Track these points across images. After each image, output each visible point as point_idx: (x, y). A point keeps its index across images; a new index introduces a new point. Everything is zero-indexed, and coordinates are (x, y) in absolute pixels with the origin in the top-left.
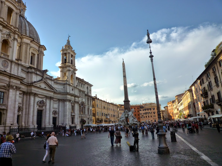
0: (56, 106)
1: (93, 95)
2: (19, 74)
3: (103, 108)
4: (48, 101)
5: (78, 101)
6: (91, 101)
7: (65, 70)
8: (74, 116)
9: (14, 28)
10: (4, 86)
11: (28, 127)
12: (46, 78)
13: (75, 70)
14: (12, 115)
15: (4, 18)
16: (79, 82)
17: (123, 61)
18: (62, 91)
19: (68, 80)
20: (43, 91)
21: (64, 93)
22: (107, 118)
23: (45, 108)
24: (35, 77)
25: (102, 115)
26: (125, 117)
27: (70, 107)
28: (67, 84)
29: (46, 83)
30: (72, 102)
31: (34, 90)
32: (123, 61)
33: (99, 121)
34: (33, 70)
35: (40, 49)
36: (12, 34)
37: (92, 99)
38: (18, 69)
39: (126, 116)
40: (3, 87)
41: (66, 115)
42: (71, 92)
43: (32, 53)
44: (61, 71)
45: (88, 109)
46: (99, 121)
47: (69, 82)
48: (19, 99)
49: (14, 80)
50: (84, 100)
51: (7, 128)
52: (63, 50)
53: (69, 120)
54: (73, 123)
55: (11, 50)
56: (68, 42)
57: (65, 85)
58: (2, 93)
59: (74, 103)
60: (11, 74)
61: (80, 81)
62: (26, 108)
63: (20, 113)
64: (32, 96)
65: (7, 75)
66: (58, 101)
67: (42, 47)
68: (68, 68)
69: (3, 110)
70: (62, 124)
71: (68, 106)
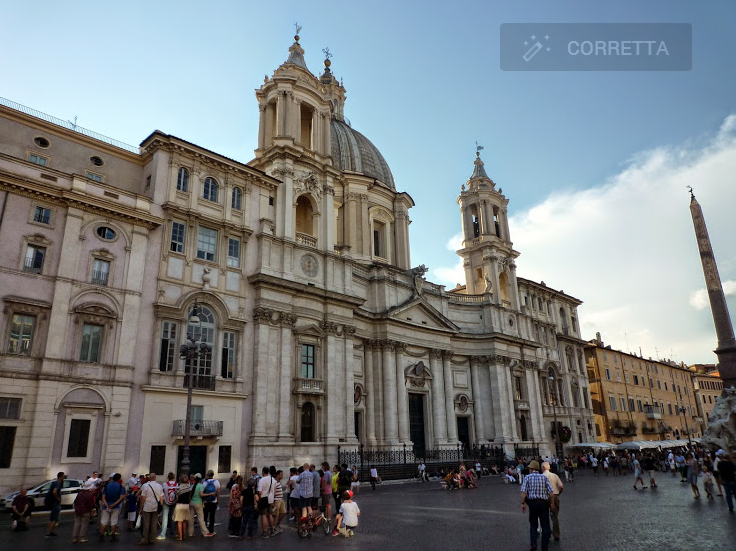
0: (462, 379)
1: (587, 335)
2: (347, 288)
3: (630, 381)
4: (437, 365)
5: (533, 360)
6: (580, 359)
7: (480, 258)
8: (527, 411)
9: (323, 158)
10: (312, 328)
11: (387, 449)
12: (425, 292)
13: (513, 254)
14: (339, 412)
15: (294, 136)
16: (528, 294)
17: (693, 197)
18: (476, 329)
19: (491, 291)
20: (420, 334)
21: (483, 334)
22: (652, 419)
23: (432, 387)
24: (393, 293)
25: (632, 409)
26: (729, 413)
27: (509, 382)
28: (489, 305)
29: (425, 308)
30: (512, 363)
31: (394, 333)
32: (693, 197)
33: (622, 432)
34: (385, 273)
35: (396, 204)
36: (317, 177)
37: (585, 349)
40: (310, 332)
41: (499, 409)
42: (508, 331)
43: (375, 221)
44: (466, 265)
45: (575, 386)
46: (622, 432)
47: (497, 300)
48: (355, 365)
49: (336, 307)
50: (554, 356)
51: (332, 451)
52: (464, 196)
53: (511, 428)
55: (318, 222)
56: (479, 166)
58: (311, 349)
59: (520, 367)
60: (326, 291)
61: (532, 292)
62: (376, 391)
63: (362, 406)
64: (389, 353)
65: (316, 295)
66: (467, 364)
67: (401, 200)
68: (487, 253)
69: (317, 396)
70: (490, 441)
71: (500, 378)
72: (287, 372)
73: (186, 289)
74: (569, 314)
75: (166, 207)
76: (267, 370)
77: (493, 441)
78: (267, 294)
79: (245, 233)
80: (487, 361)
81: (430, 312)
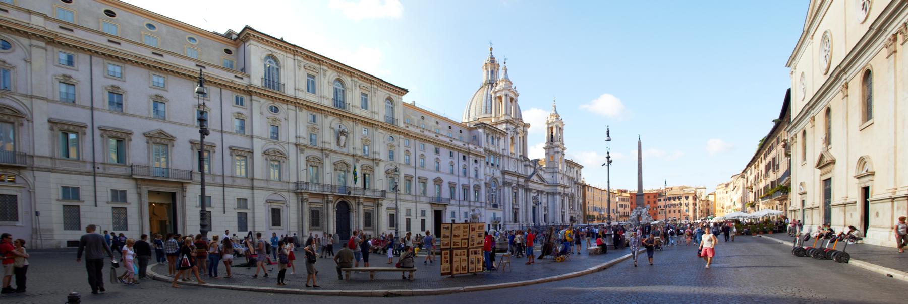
5: (567, 193)
8: (564, 212)
10: (517, 187)
13: (564, 149)
16: (567, 165)
18: (550, 181)
31: (531, 185)
35: (525, 128)
38: (522, 165)
39: (639, 213)
42: (562, 182)
44: (546, 154)
45: (578, 202)
47: (558, 169)
50: (573, 191)
51: (521, 226)
54: (563, 222)
57: (555, 174)
60: (519, 174)
66: (547, 195)
67: (527, 126)
71: (558, 200)
72: (511, 202)
73: (490, 177)
74: (579, 172)
75: (485, 150)
76: (507, 201)
78: (507, 176)
79: (500, 155)
80: (554, 194)
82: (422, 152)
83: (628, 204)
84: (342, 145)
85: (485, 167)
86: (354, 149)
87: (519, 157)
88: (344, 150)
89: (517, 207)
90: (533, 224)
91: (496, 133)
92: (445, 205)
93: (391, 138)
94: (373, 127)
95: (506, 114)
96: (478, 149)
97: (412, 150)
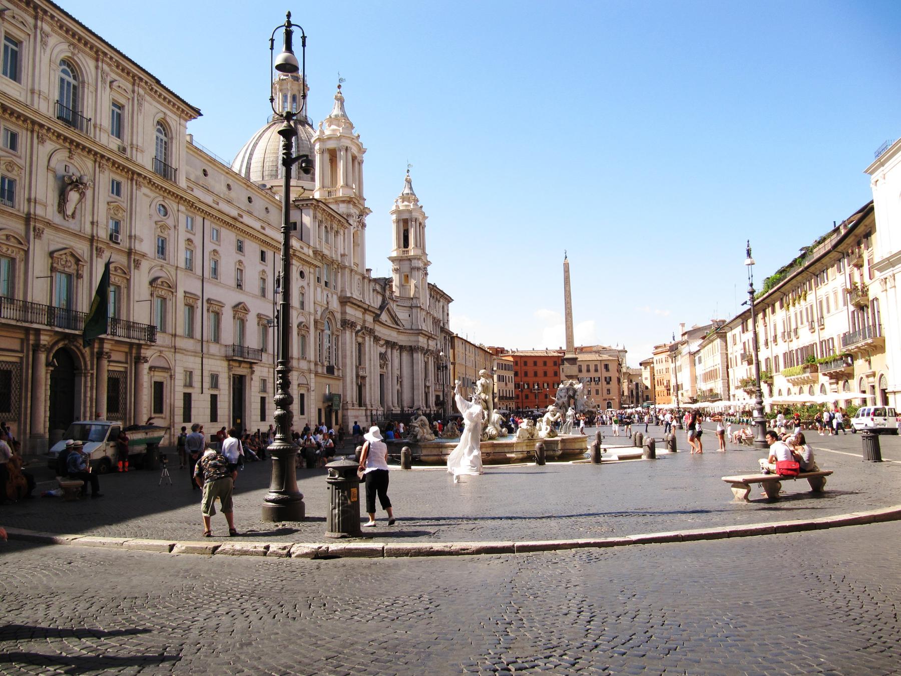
8: (428, 387)
13: (427, 263)
16: (431, 295)
17: (566, 257)
26: (567, 395)
28: (417, 307)
31: (380, 331)
54: (427, 408)
57: (414, 310)
66: (399, 351)
73: (323, 308)
75: (316, 252)
76: (348, 361)
77: (411, 408)
78: (349, 310)
80: (412, 350)
81: (391, 314)
82: (216, 247)
83: (510, 374)
84: (69, 212)
85: (315, 289)
86: (92, 223)
87: (365, 273)
88: (72, 225)
89: (364, 374)
90: (382, 409)
91: (332, 221)
92: (251, 363)
93: (162, 208)
94: (132, 180)
95: (347, 185)
96: (306, 250)
97: (197, 240)
